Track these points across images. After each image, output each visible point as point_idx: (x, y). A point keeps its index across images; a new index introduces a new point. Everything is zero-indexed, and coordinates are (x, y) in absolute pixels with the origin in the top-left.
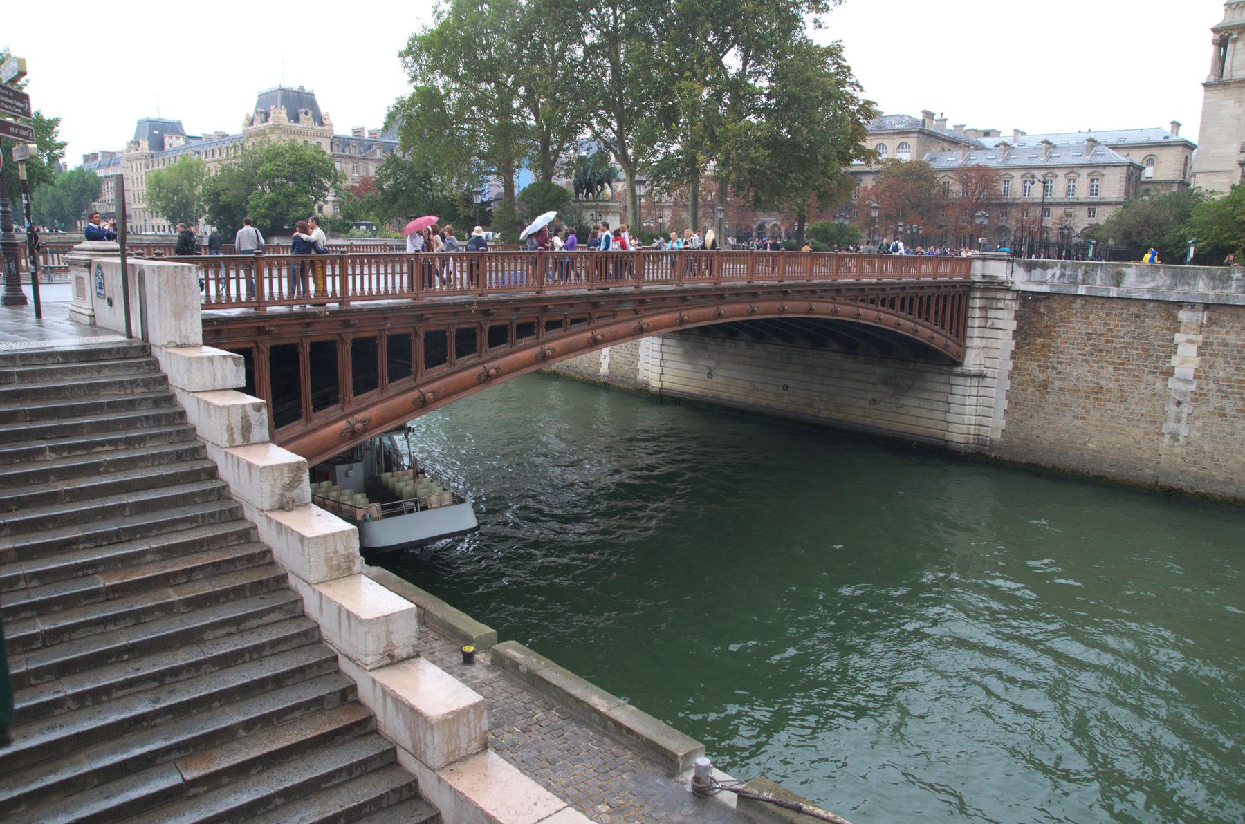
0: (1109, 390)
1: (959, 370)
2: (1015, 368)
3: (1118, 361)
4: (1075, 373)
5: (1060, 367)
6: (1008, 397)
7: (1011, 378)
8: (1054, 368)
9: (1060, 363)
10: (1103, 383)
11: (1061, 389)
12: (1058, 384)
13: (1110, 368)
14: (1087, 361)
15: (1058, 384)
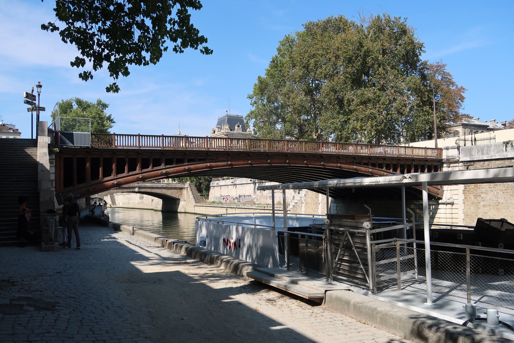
0: (502, 203)
1: (440, 201)
2: (465, 198)
3: (504, 189)
4: (488, 197)
5: (483, 195)
6: (464, 213)
7: (464, 203)
8: (480, 196)
9: (482, 193)
10: (499, 201)
11: (484, 206)
12: (482, 203)
13: (501, 193)
14: (491, 191)
15: (482, 203)
